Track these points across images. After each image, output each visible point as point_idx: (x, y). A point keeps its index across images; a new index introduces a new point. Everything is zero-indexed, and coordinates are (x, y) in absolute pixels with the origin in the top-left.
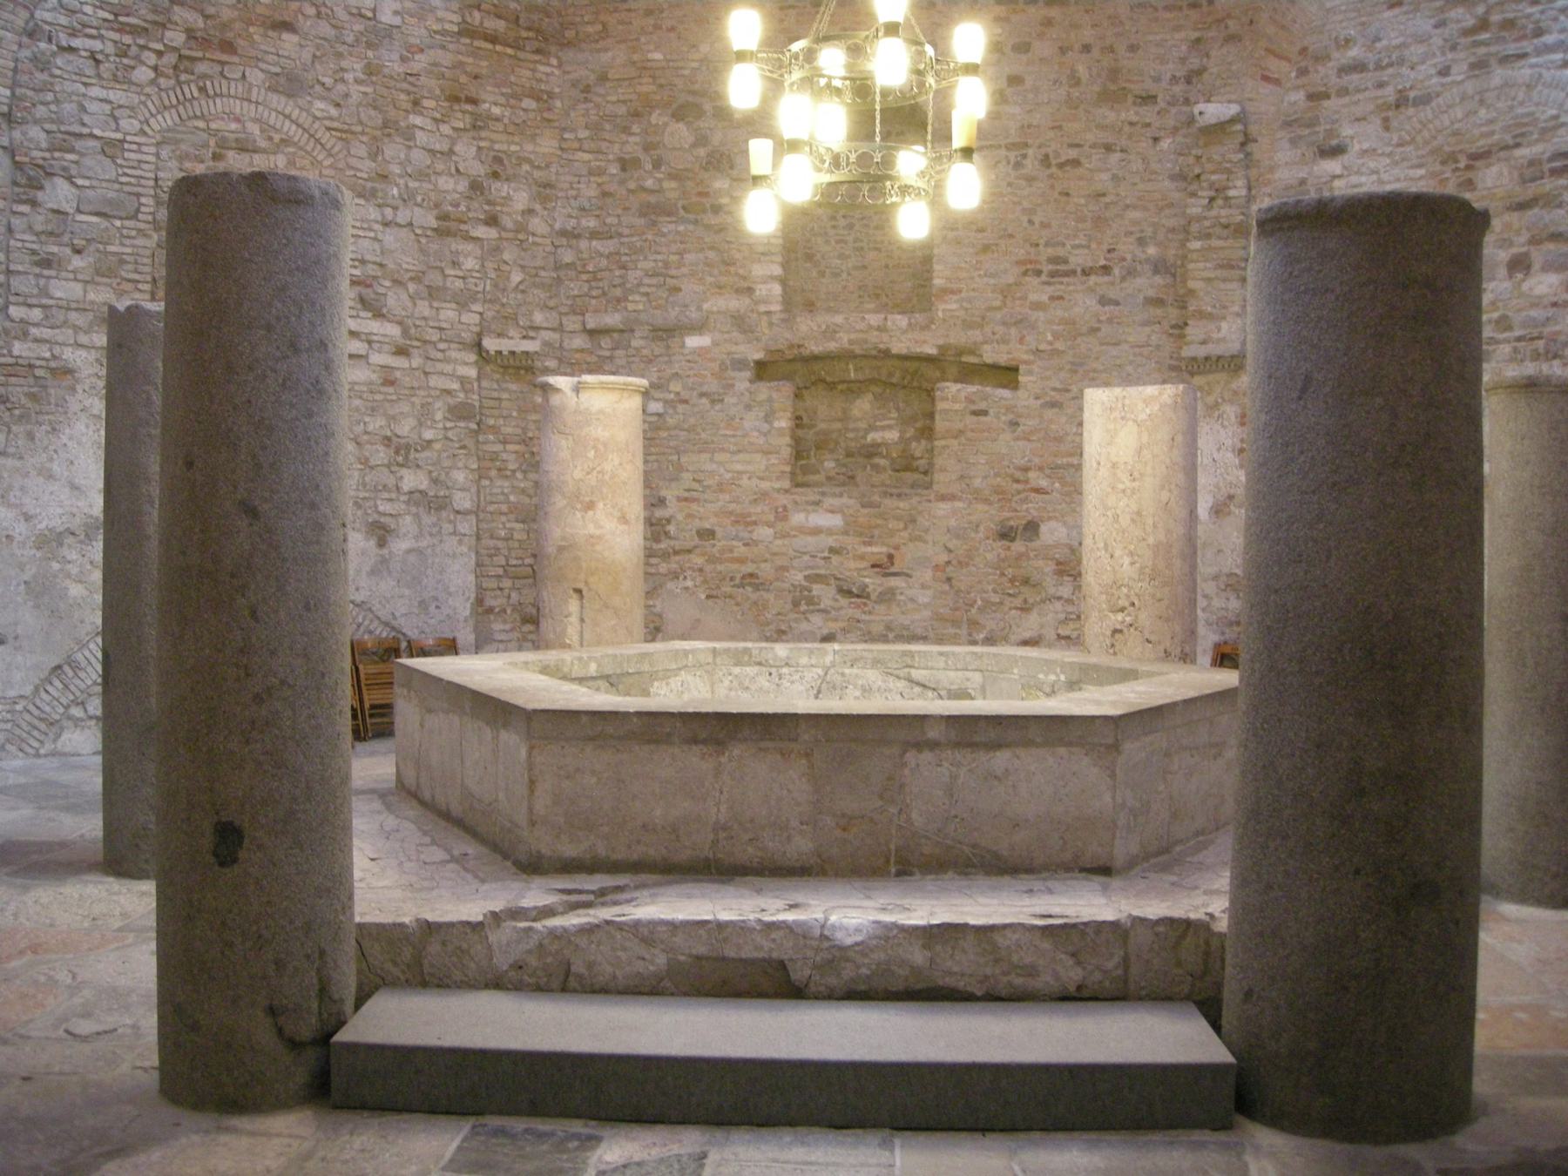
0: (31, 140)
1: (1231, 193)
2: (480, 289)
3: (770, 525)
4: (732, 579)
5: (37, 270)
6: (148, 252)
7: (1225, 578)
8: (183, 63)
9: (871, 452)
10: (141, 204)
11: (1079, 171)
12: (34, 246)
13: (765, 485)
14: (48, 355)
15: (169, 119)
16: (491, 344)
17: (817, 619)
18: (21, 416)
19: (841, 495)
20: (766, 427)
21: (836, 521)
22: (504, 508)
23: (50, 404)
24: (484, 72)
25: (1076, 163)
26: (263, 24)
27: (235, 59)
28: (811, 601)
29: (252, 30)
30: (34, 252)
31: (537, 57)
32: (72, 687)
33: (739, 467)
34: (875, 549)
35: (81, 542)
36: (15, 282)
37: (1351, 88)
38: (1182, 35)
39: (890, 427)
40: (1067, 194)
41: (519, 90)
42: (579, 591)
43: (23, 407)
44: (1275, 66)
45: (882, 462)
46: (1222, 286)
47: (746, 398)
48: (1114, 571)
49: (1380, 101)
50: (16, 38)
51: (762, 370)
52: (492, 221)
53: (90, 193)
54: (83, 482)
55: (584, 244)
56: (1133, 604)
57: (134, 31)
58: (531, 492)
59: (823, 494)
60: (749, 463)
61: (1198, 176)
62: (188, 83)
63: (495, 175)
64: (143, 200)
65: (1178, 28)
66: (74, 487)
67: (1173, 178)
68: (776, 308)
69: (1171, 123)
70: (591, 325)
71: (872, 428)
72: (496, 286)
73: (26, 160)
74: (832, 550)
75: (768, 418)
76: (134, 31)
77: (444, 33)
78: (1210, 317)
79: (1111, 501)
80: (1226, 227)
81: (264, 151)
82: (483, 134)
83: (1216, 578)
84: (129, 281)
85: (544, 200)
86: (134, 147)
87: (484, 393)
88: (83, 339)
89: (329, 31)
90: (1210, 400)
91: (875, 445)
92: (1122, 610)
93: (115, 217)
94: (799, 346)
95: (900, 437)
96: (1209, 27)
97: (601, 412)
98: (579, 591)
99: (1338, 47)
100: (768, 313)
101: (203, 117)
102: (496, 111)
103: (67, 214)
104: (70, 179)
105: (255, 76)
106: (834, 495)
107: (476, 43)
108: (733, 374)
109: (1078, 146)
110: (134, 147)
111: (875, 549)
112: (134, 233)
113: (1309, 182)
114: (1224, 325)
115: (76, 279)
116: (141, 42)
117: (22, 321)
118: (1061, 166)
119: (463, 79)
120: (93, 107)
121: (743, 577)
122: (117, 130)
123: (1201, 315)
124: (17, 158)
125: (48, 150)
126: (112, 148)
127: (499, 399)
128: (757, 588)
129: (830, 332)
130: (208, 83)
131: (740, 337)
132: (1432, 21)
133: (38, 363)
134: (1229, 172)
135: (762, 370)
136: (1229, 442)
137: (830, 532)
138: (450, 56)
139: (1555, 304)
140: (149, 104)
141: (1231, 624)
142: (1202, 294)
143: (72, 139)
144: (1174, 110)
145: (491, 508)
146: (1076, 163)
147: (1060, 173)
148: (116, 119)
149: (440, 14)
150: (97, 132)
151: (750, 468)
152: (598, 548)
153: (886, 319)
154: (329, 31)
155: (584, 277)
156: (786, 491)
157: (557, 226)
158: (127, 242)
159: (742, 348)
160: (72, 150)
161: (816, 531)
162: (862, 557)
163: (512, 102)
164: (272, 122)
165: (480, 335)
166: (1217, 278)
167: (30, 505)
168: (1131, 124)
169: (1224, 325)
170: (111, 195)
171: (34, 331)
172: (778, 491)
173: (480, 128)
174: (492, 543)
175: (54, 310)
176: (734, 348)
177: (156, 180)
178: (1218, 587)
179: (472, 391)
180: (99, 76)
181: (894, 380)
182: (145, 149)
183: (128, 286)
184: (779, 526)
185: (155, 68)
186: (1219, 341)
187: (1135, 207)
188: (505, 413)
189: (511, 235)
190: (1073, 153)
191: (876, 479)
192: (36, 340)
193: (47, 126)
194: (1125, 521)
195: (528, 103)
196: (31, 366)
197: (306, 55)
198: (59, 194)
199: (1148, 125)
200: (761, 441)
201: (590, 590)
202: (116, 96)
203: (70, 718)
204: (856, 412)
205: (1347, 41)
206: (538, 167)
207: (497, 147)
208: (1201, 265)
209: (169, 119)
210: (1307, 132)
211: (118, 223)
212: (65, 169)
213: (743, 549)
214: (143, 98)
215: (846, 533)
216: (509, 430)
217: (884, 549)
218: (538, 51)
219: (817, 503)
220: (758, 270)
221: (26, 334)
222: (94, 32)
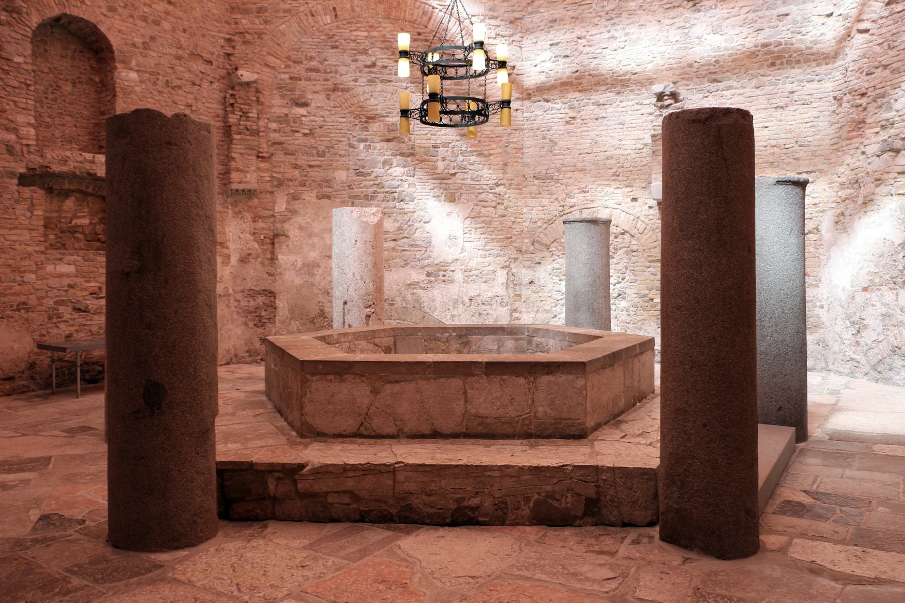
1: (250, 115)
3: (35, 273)
4: (11, 306)
7: (247, 292)
9: (74, 230)
11: (181, 92)
13: (30, 249)
17: (63, 326)
19: (73, 255)
20: (28, 214)
21: (71, 269)
25: (180, 87)
28: (59, 316)
33: (14, 238)
34: (92, 284)
37: (312, 78)
38: (222, 35)
39: (84, 216)
40: (176, 103)
44: (271, 60)
45: (80, 236)
47: (16, 196)
49: (326, 87)
51: (24, 180)
59: (64, 254)
60: (20, 235)
61: (232, 105)
65: (220, 31)
68: (33, 143)
69: (217, 77)
71: (76, 217)
74: (70, 286)
75: (31, 207)
78: (241, 171)
80: (248, 129)
83: (242, 292)
90: (237, 209)
91: (77, 226)
92: (369, 306)
94: (47, 167)
95: (91, 223)
99: (306, 59)
100: (28, 145)
106: (70, 254)
108: (7, 180)
109: (181, 79)
111: (92, 284)
113: (290, 116)
114: (249, 175)
118: (173, 88)
121: (18, 305)
123: (238, 170)
128: (27, 310)
129: (65, 161)
131: (11, 158)
132: (352, 58)
134: (249, 104)
135: (24, 180)
136: (248, 229)
137: (68, 276)
141: (251, 312)
142: (238, 160)
144: (219, 70)
146: (180, 87)
147: (172, 92)
151: (21, 238)
153: (94, 157)
156: (42, 252)
159: (13, 165)
161: (61, 276)
162: (86, 290)
166: (245, 153)
168: (202, 73)
169: (249, 175)
172: (37, 252)
176: (7, 165)
178: (243, 296)
181: (90, 191)
184: (40, 272)
186: (246, 183)
187: (204, 115)
190: (179, 82)
191: (77, 245)
199: (209, 75)
200: (27, 222)
204: (66, 207)
205: (311, 58)
208: (239, 146)
210: (289, 93)
213: (18, 288)
215: (77, 276)
217: (97, 285)
219: (60, 260)
220: (21, 118)
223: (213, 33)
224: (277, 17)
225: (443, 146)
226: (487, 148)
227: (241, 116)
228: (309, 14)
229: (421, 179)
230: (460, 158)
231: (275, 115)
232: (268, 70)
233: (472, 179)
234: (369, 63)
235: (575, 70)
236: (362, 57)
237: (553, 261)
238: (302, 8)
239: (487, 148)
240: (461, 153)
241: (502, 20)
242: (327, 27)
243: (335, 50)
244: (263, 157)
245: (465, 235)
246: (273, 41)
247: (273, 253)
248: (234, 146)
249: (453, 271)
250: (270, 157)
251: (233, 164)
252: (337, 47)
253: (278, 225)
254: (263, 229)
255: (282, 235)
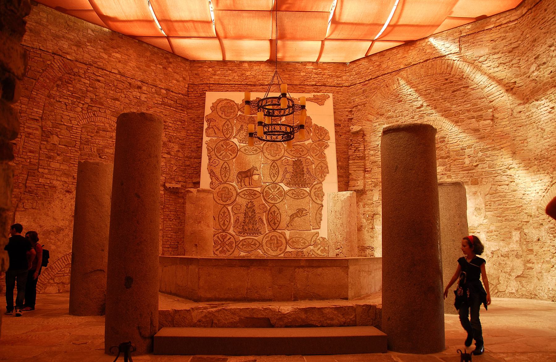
0: (47, 125)
1: (360, 149)
2: (165, 171)
5: (47, 159)
6: (78, 156)
8: (90, 107)
10: (76, 143)
12: (47, 153)
14: (49, 182)
15: (85, 121)
16: (168, 185)
18: (41, 199)
22: (170, 229)
23: (49, 195)
24: (168, 114)
26: (111, 98)
27: (103, 107)
29: (108, 100)
30: (47, 154)
31: (181, 111)
32: (50, 274)
35: (56, 234)
36: (41, 162)
41: (176, 119)
42: (196, 245)
43: (41, 196)
46: (358, 172)
48: (336, 239)
50: (45, 98)
52: (169, 153)
53: (63, 139)
54: (57, 217)
55: (192, 160)
56: (341, 247)
57: (77, 98)
58: (177, 225)
61: (351, 144)
62: (90, 112)
63: (170, 141)
64: (77, 142)
66: (54, 219)
67: (345, 145)
70: (194, 181)
72: (169, 170)
73: (46, 130)
76: (77, 98)
77: (157, 104)
79: (335, 221)
81: (109, 132)
82: (167, 130)
84: (72, 164)
85: (182, 148)
86: (75, 128)
87: (165, 198)
88: (59, 179)
89: (128, 101)
92: (339, 249)
93: (69, 146)
96: (353, 108)
97: (203, 198)
98: (196, 245)
101: (94, 122)
102: (170, 125)
103: (56, 145)
104: (57, 136)
105: (108, 112)
107: (166, 107)
110: (75, 128)
112: (74, 151)
115: (58, 162)
116: (79, 101)
117: (42, 173)
119: (162, 116)
120: (65, 117)
122: (71, 123)
124: (43, 129)
125: (52, 128)
126: (69, 129)
127: (170, 200)
130: (96, 113)
133: (46, 184)
138: (159, 109)
139: (442, 174)
140: (80, 117)
143: (59, 125)
144: (345, 128)
145: (167, 229)
148: (71, 121)
149: (157, 99)
150: (65, 124)
152: (202, 233)
154: (128, 101)
155: (193, 168)
157: (185, 155)
158: (72, 153)
160: (59, 128)
163: (175, 122)
164: (112, 124)
165: (165, 183)
166: (357, 170)
167: (41, 223)
169: (359, 182)
170: (68, 140)
171: (45, 175)
173: (166, 129)
174: (167, 238)
175: (51, 170)
177: (81, 137)
179: (162, 197)
180: (66, 109)
182: (78, 129)
183: (72, 165)
185: (82, 108)
188: (171, 204)
189: (173, 157)
192: (46, 178)
193: (52, 121)
194: (339, 226)
195: (179, 123)
196: (44, 185)
197: (122, 108)
198: (55, 139)
201: (199, 244)
202: (72, 115)
203: (49, 283)
206: (181, 140)
207: (170, 134)
209: (85, 121)
211: (70, 148)
212: (56, 133)
214: (78, 116)
216: (172, 208)
218: (181, 110)
221: (43, 176)
222: (66, 97)
223: (341, 110)
224: (371, 93)
225: (468, 148)
226: (499, 144)
227: (355, 150)
228: (386, 86)
229: (454, 172)
230: (480, 154)
231: (372, 146)
232: (368, 122)
233: (489, 167)
234: (419, 106)
235: (550, 71)
236: (415, 103)
237: (549, 221)
238: (382, 85)
239: (499, 144)
240: (480, 151)
241: (502, 53)
242: (395, 91)
243: (400, 103)
244: (367, 171)
245: (486, 207)
246: (370, 106)
247: (373, 225)
248: (350, 167)
249: (479, 233)
250: (371, 171)
251: (351, 177)
252: (401, 101)
253: (375, 208)
254: (368, 211)
255: (377, 214)
